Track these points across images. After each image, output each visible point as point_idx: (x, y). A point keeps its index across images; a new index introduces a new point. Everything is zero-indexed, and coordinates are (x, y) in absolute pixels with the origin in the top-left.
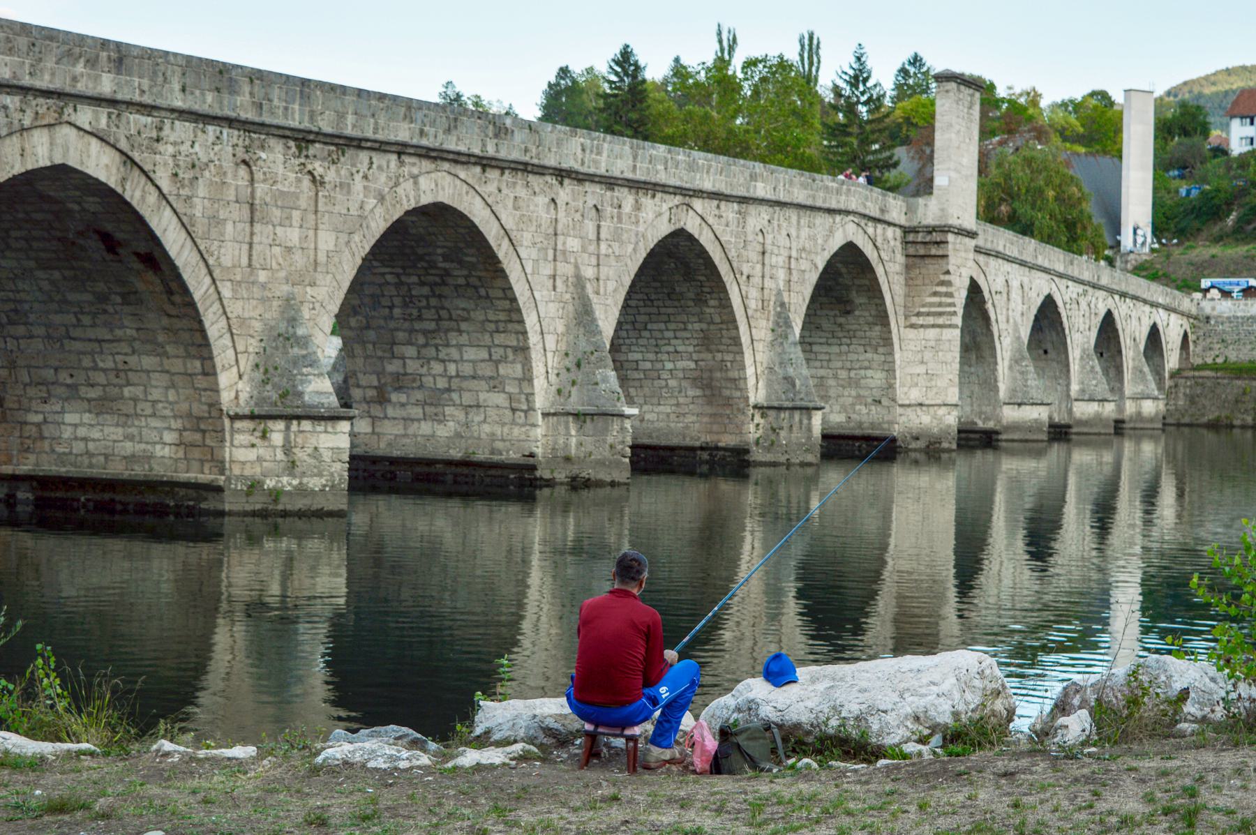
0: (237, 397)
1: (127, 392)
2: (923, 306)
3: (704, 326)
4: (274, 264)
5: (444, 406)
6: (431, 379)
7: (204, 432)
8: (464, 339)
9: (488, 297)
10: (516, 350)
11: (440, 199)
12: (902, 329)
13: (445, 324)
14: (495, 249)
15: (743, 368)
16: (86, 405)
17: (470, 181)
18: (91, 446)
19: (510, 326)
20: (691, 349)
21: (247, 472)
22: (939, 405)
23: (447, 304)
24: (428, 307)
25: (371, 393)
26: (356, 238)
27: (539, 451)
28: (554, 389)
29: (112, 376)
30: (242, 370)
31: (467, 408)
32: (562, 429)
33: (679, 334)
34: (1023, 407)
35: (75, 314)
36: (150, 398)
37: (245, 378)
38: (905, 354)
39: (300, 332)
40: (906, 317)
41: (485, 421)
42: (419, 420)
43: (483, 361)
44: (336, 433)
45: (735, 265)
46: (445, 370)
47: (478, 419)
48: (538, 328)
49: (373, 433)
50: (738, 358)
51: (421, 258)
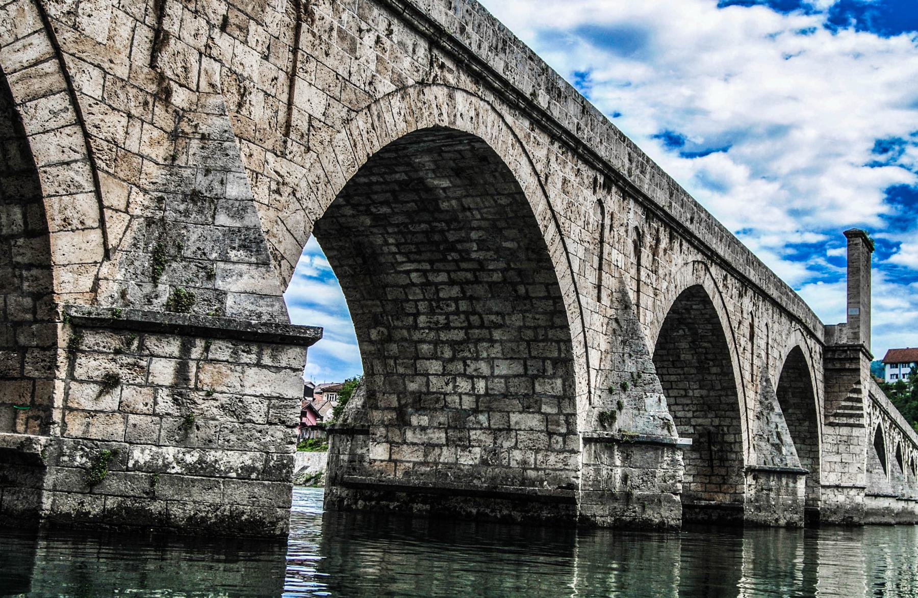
0: (95, 289)
2: (840, 408)
3: (704, 392)
4: (204, 86)
5: (470, 429)
6: (457, 399)
8: (496, 351)
9: (527, 297)
10: (555, 362)
11: (480, 133)
14: (542, 229)
17: (517, 132)
19: (550, 334)
20: (690, 415)
21: (96, 432)
22: (851, 488)
23: (479, 308)
24: (457, 312)
25: (389, 416)
27: (580, 482)
28: (596, 412)
30: (112, 241)
31: (495, 432)
33: (679, 401)
34: (878, 499)
37: (118, 257)
38: (825, 445)
39: (233, 190)
40: (826, 417)
41: (515, 447)
42: (440, 446)
43: (515, 376)
44: (278, 369)
45: (736, 335)
46: (473, 388)
47: (506, 444)
48: (581, 338)
49: (390, 460)
50: (735, 423)
51: (452, 248)
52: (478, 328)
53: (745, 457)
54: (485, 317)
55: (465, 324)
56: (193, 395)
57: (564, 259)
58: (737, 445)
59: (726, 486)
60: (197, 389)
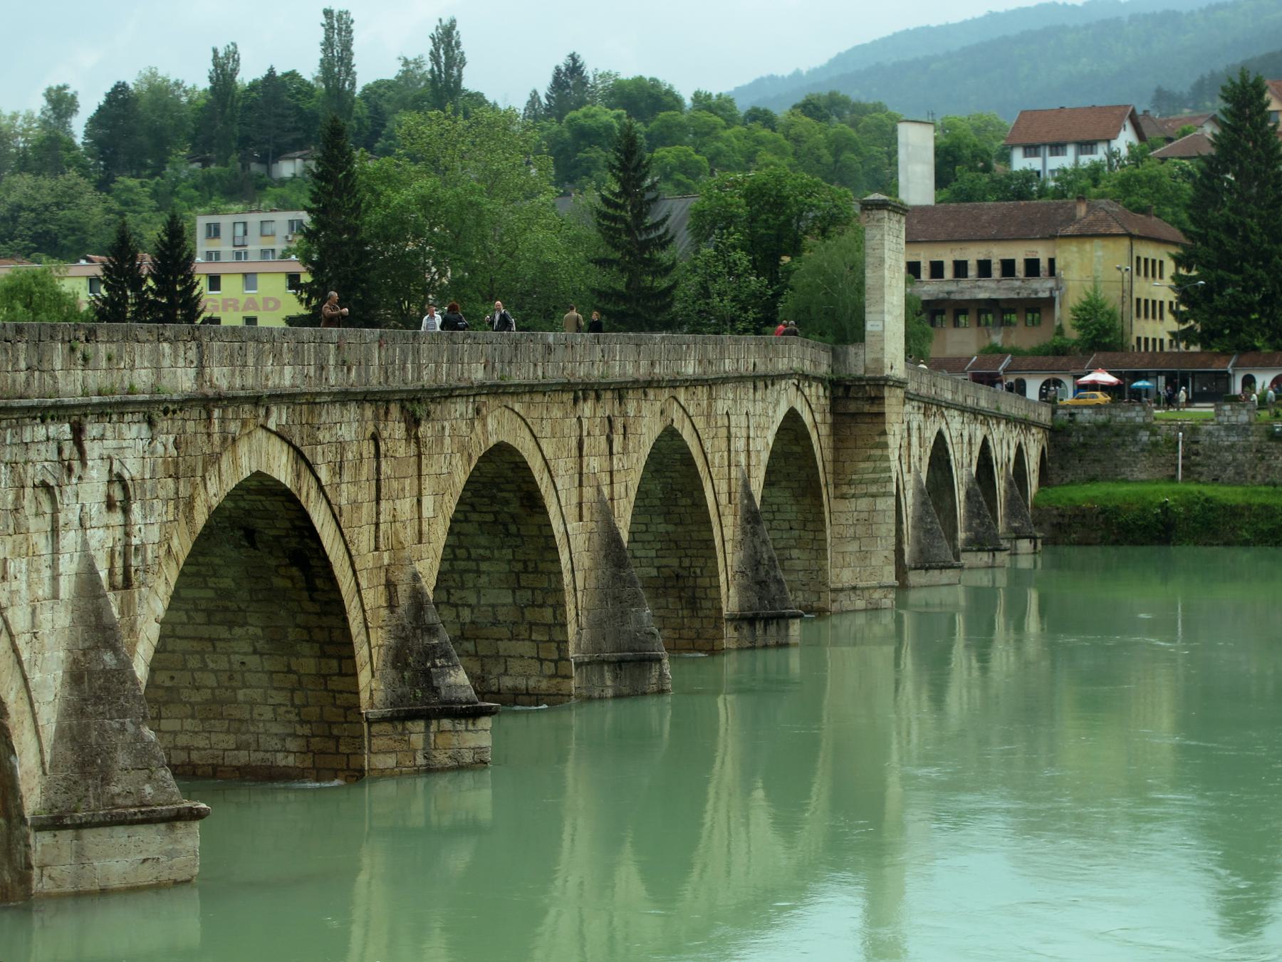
1: (241, 695)
7: (337, 738)
9: (518, 535)
12: (832, 500)
13: (461, 565)
15: (717, 576)
16: (188, 709)
18: (195, 756)
20: (653, 553)
22: (874, 588)
26: (447, 498)
29: (224, 677)
32: (595, 679)
34: (931, 572)
35: (187, 611)
36: (271, 701)
37: (377, 674)
38: (836, 529)
41: (506, 673)
44: (477, 731)
46: (458, 616)
48: (569, 566)
52: (464, 560)
53: (724, 606)
54: (473, 551)
55: (452, 556)
56: (434, 753)
57: (555, 500)
58: (713, 591)
59: (701, 642)
60: (435, 749)
